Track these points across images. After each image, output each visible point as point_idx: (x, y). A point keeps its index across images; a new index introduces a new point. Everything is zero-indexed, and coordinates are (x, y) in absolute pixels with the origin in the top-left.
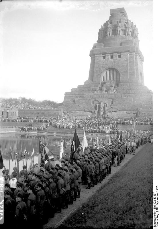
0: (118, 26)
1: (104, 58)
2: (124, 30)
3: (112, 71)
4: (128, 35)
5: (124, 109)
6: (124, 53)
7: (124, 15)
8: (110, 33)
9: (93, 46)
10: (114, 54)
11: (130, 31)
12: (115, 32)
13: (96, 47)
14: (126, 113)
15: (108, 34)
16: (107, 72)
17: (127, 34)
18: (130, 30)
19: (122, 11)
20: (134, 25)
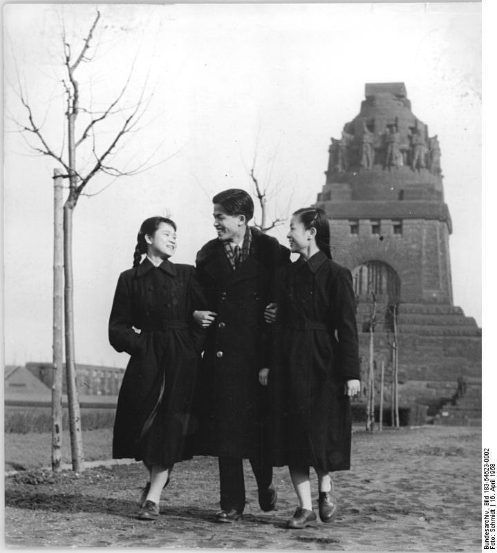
0: (392, 142)
1: (355, 229)
2: (408, 152)
3: (375, 267)
4: (419, 166)
5: (421, 377)
6: (411, 221)
7: (402, 103)
8: (370, 156)
9: (320, 190)
10: (383, 222)
11: (421, 151)
12: (383, 156)
13: (332, 196)
14: (428, 386)
15: (364, 162)
16: (361, 271)
17: (415, 163)
18: (425, 150)
19: (398, 92)
20: (431, 135)
